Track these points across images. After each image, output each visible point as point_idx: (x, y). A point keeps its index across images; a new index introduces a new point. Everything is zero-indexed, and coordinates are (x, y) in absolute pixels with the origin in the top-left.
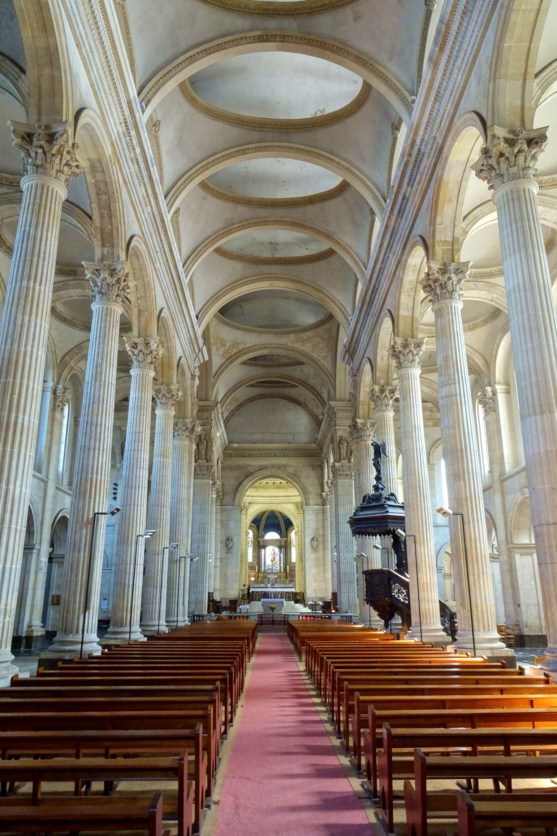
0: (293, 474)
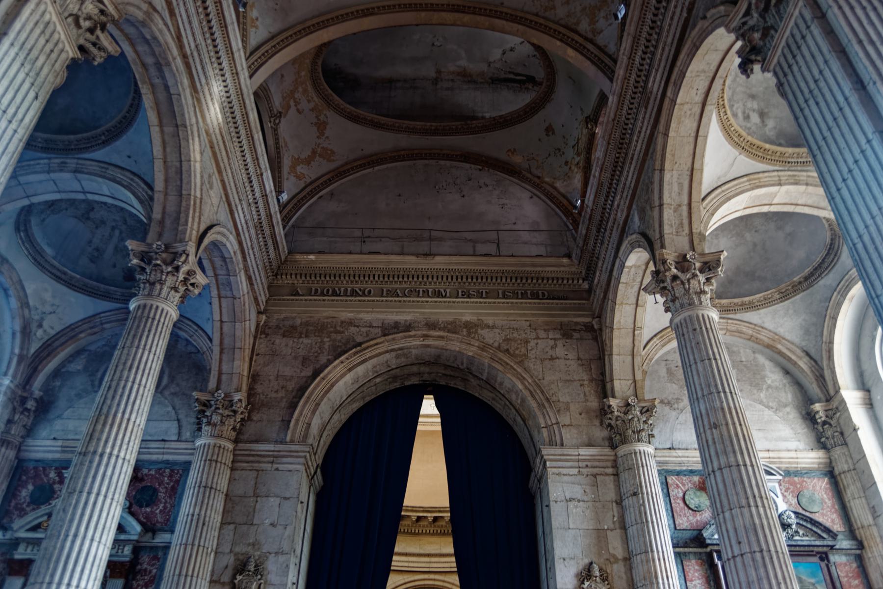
0: (499, 348)
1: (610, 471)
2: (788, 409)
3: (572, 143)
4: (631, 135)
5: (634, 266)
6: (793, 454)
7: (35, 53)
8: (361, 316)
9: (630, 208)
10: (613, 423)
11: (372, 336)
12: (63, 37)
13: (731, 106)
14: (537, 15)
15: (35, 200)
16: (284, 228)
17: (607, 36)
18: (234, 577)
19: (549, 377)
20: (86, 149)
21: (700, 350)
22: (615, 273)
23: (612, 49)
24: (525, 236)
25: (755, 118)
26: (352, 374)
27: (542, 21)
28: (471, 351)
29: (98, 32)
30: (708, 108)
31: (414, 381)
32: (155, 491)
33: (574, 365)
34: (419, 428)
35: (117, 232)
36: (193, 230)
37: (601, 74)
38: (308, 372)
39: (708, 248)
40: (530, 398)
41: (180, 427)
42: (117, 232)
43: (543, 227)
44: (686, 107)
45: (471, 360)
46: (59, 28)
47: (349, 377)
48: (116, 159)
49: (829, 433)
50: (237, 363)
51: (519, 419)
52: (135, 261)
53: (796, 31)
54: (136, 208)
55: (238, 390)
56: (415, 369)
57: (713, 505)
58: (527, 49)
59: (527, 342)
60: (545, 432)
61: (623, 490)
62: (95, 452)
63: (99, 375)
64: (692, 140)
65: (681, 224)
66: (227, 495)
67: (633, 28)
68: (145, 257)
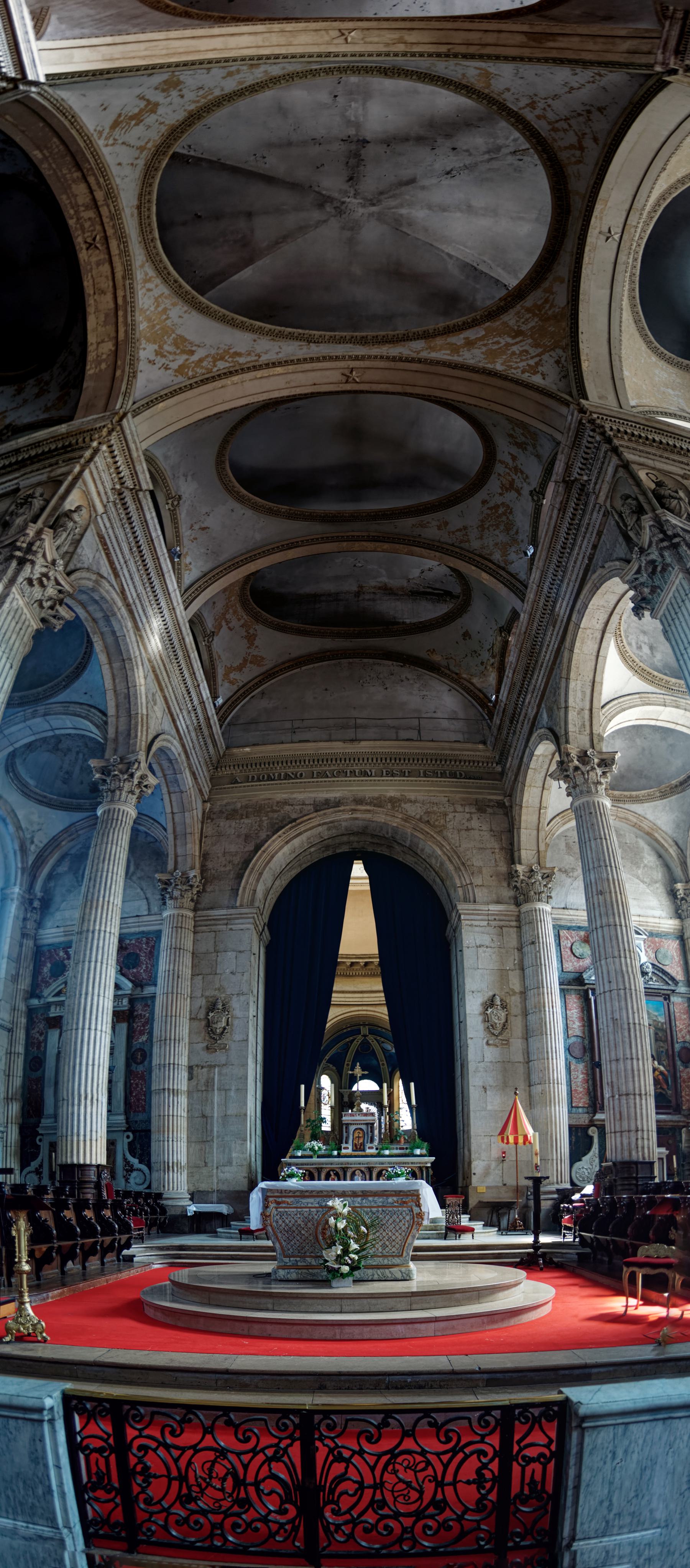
1: (514, 924)
2: (658, 885)
3: (487, 646)
4: (541, 646)
5: (542, 755)
6: (657, 920)
7: (8, 634)
8: (294, 796)
9: (539, 706)
10: (518, 885)
11: (305, 812)
12: (29, 616)
13: (627, 637)
14: (453, 545)
15: (17, 745)
16: (221, 726)
17: (518, 566)
18: (207, 1014)
19: (465, 845)
20: (51, 696)
21: (594, 831)
22: (525, 760)
23: (522, 576)
24: (445, 724)
25: (646, 649)
26: (289, 846)
27: (457, 550)
28: (395, 822)
29: (58, 607)
30: (607, 635)
31: (345, 849)
32: (138, 956)
33: (486, 835)
34: (350, 888)
35: (81, 756)
36: (142, 742)
37: (512, 595)
38: (251, 847)
39: (605, 748)
40: (448, 862)
41: (149, 904)
42: (81, 756)
43: (461, 715)
44: (588, 632)
45: (395, 830)
46: (25, 611)
47: (286, 849)
48: (75, 698)
49: (684, 907)
50: (189, 846)
51: (438, 880)
52: (97, 776)
53: (677, 595)
54: (94, 732)
55: (193, 868)
56: (345, 839)
57: (593, 954)
58: (444, 570)
59: (445, 815)
60: (460, 891)
61: (524, 939)
62: (88, 931)
63: (81, 872)
64: (594, 658)
65: (584, 725)
66: (193, 953)
67: (541, 564)
68: (105, 771)
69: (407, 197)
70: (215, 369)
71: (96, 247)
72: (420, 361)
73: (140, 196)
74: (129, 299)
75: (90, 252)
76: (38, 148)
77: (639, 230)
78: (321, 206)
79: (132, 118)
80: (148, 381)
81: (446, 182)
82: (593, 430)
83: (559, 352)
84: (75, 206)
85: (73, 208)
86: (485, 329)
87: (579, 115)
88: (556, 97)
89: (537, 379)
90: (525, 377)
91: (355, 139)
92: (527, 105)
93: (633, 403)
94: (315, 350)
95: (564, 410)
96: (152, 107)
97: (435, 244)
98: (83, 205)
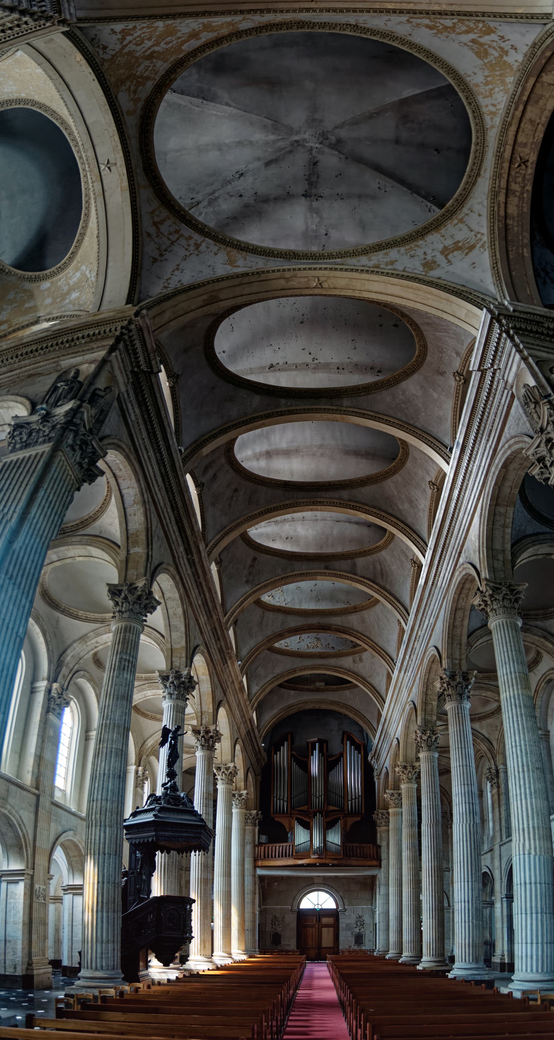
69: (270, 150)
70: (455, 21)
71: (521, 158)
72: (242, 12)
73: (474, 184)
74: (513, 106)
75: (527, 158)
76: (523, 257)
77: (90, 181)
78: (339, 141)
79: (460, 248)
80: (523, 35)
81: (242, 167)
82: (43, 12)
83: (106, 57)
84: (521, 198)
85: (523, 198)
86: (183, 51)
87: (166, 250)
88: (185, 258)
89: (119, 27)
90: (131, 25)
91: (312, 198)
92: (200, 245)
93: (19, 53)
94: (351, 19)
95: (81, 14)
96: (445, 252)
97: (243, 113)
98: (516, 196)
